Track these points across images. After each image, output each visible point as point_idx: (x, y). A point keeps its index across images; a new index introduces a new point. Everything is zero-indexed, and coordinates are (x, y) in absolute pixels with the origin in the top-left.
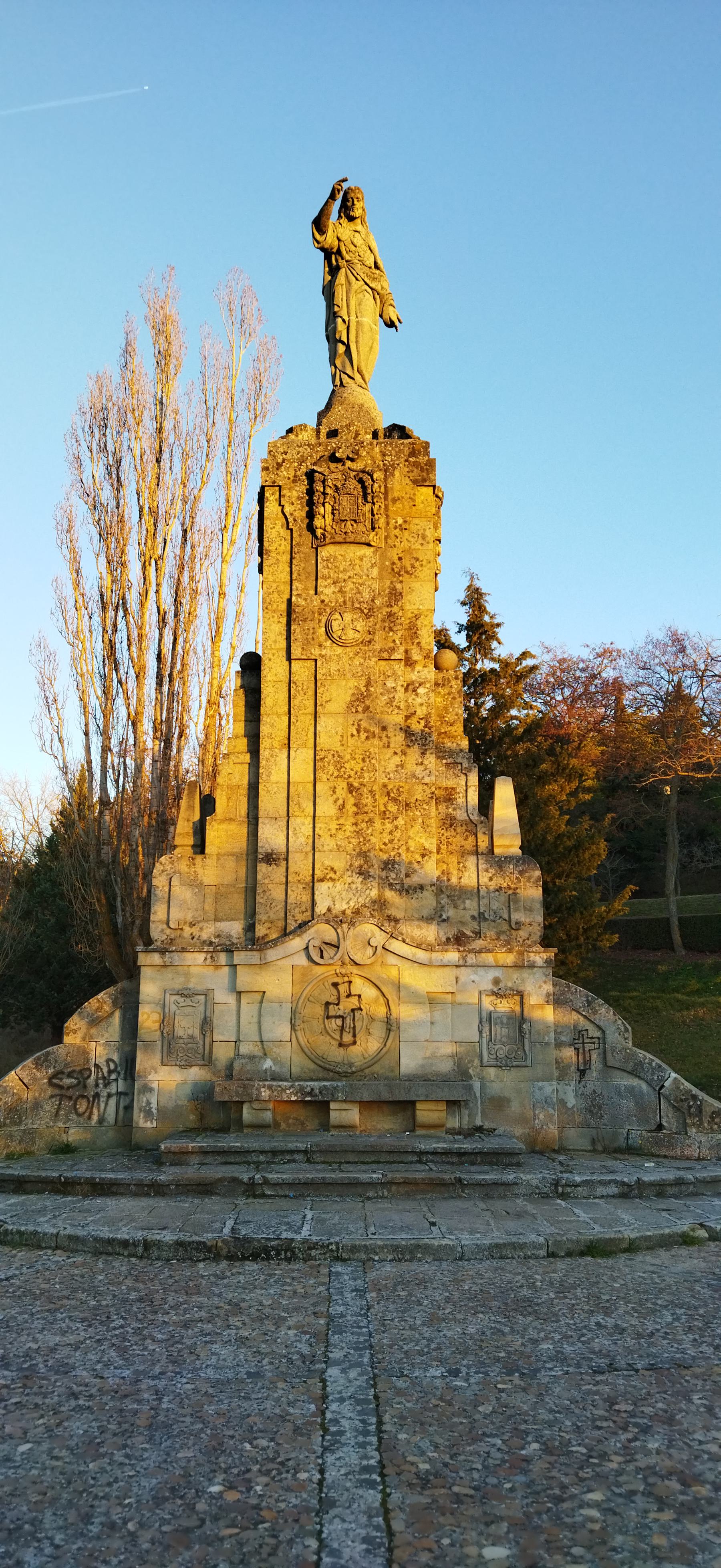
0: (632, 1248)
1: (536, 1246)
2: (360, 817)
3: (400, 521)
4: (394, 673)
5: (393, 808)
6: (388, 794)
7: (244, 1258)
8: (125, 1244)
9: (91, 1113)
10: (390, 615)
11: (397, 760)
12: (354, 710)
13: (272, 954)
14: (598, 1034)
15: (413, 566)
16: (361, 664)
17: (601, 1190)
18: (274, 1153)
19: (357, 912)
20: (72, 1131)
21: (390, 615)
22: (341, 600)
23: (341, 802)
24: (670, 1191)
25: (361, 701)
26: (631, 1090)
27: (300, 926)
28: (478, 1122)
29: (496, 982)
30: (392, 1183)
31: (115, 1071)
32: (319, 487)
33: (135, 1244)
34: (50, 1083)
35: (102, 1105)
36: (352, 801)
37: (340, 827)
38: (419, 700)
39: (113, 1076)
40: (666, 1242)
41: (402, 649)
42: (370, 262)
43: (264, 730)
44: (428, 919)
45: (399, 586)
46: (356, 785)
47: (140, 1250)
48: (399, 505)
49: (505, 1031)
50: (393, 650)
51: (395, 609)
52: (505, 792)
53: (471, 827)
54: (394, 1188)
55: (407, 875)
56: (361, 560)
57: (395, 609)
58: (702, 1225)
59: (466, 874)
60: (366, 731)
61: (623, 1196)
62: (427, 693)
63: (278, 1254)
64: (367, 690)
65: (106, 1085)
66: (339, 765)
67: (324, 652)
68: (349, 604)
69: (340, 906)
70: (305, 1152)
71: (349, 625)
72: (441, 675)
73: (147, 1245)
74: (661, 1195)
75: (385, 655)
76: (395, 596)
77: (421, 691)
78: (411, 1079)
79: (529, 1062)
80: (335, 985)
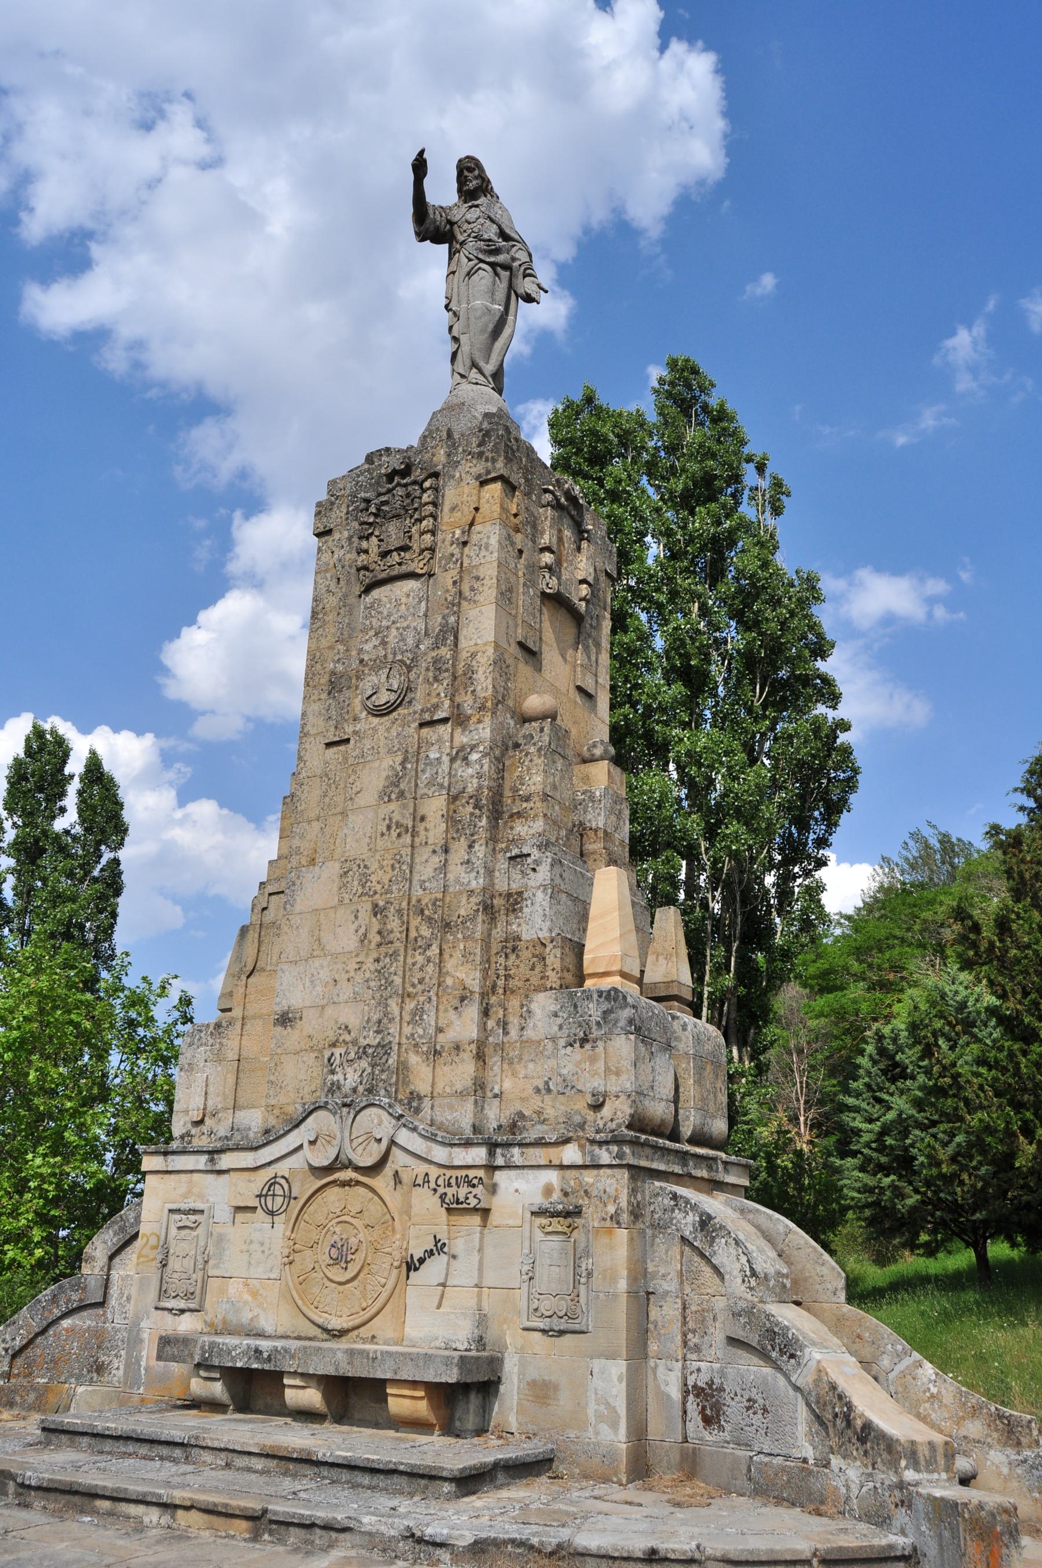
2: (383, 950)
11: (436, 860)
15: (472, 589)
16: (399, 734)
23: (362, 930)
25: (394, 788)
36: (376, 926)
46: (381, 903)
50: (436, 707)
53: (539, 949)
60: (398, 825)
64: (404, 768)
75: (427, 717)
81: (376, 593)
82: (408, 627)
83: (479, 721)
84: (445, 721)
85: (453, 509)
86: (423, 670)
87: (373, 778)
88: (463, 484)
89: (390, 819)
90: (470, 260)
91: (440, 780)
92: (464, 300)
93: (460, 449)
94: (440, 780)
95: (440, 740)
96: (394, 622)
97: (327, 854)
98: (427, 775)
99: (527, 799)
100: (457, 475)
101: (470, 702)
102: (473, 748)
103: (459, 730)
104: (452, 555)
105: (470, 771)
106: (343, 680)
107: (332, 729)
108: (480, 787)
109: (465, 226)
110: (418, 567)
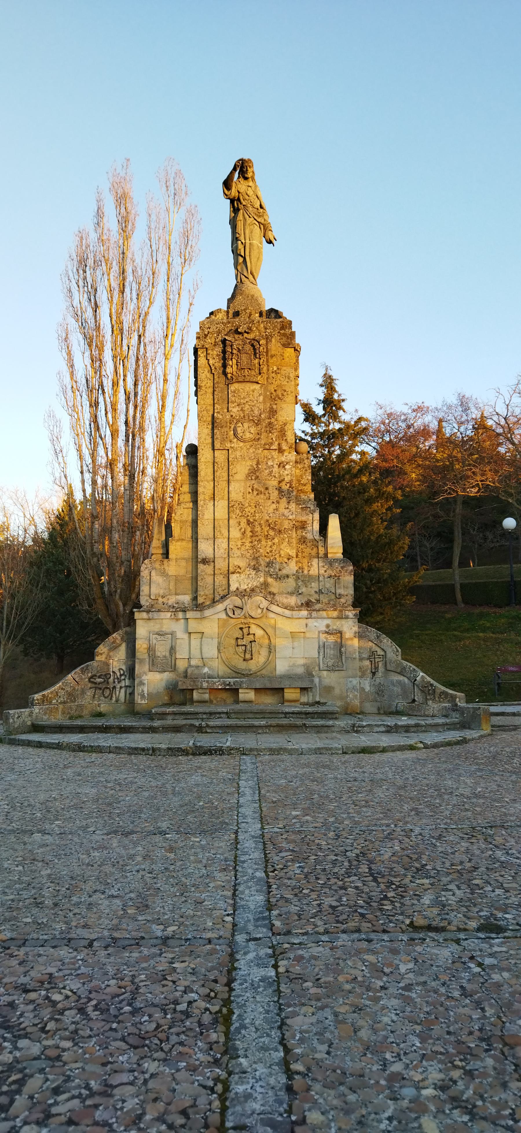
0: (384, 750)
1: (336, 749)
2: (254, 538)
3: (275, 368)
4: (272, 457)
5: (272, 533)
6: (269, 525)
7: (200, 754)
8: (143, 749)
9: (112, 696)
10: (270, 423)
11: (274, 506)
13: (207, 613)
14: (382, 653)
15: (283, 395)
17: (376, 729)
18: (211, 714)
19: (253, 590)
20: (102, 706)
21: (270, 423)
22: (242, 415)
23: (243, 530)
24: (412, 729)
25: (254, 473)
26: (399, 682)
27: (222, 598)
28: (318, 699)
29: (328, 626)
30: (271, 726)
31: (123, 674)
32: (229, 349)
33: (148, 750)
34: (90, 681)
35: (118, 693)
36: (249, 529)
37: (243, 544)
38: (286, 472)
39: (123, 677)
40: (401, 748)
41: (276, 443)
42: (258, 205)
43: (200, 490)
44: (291, 594)
45: (275, 407)
47: (151, 752)
48: (274, 359)
49: (332, 652)
50: (272, 444)
51: (273, 420)
52: (334, 522)
53: (315, 543)
54: (272, 728)
55: (280, 570)
57: (273, 420)
58: (421, 742)
59: (312, 569)
60: (257, 490)
61: (388, 732)
62: (291, 469)
63: (216, 752)
65: (119, 682)
66: (242, 510)
68: (247, 417)
69: (244, 587)
70: (227, 713)
71: (247, 430)
72: (299, 457)
73: (154, 750)
74: (407, 731)
75: (267, 447)
76: (273, 412)
77: (287, 467)
78: (282, 677)
79: (344, 668)
80: (241, 629)
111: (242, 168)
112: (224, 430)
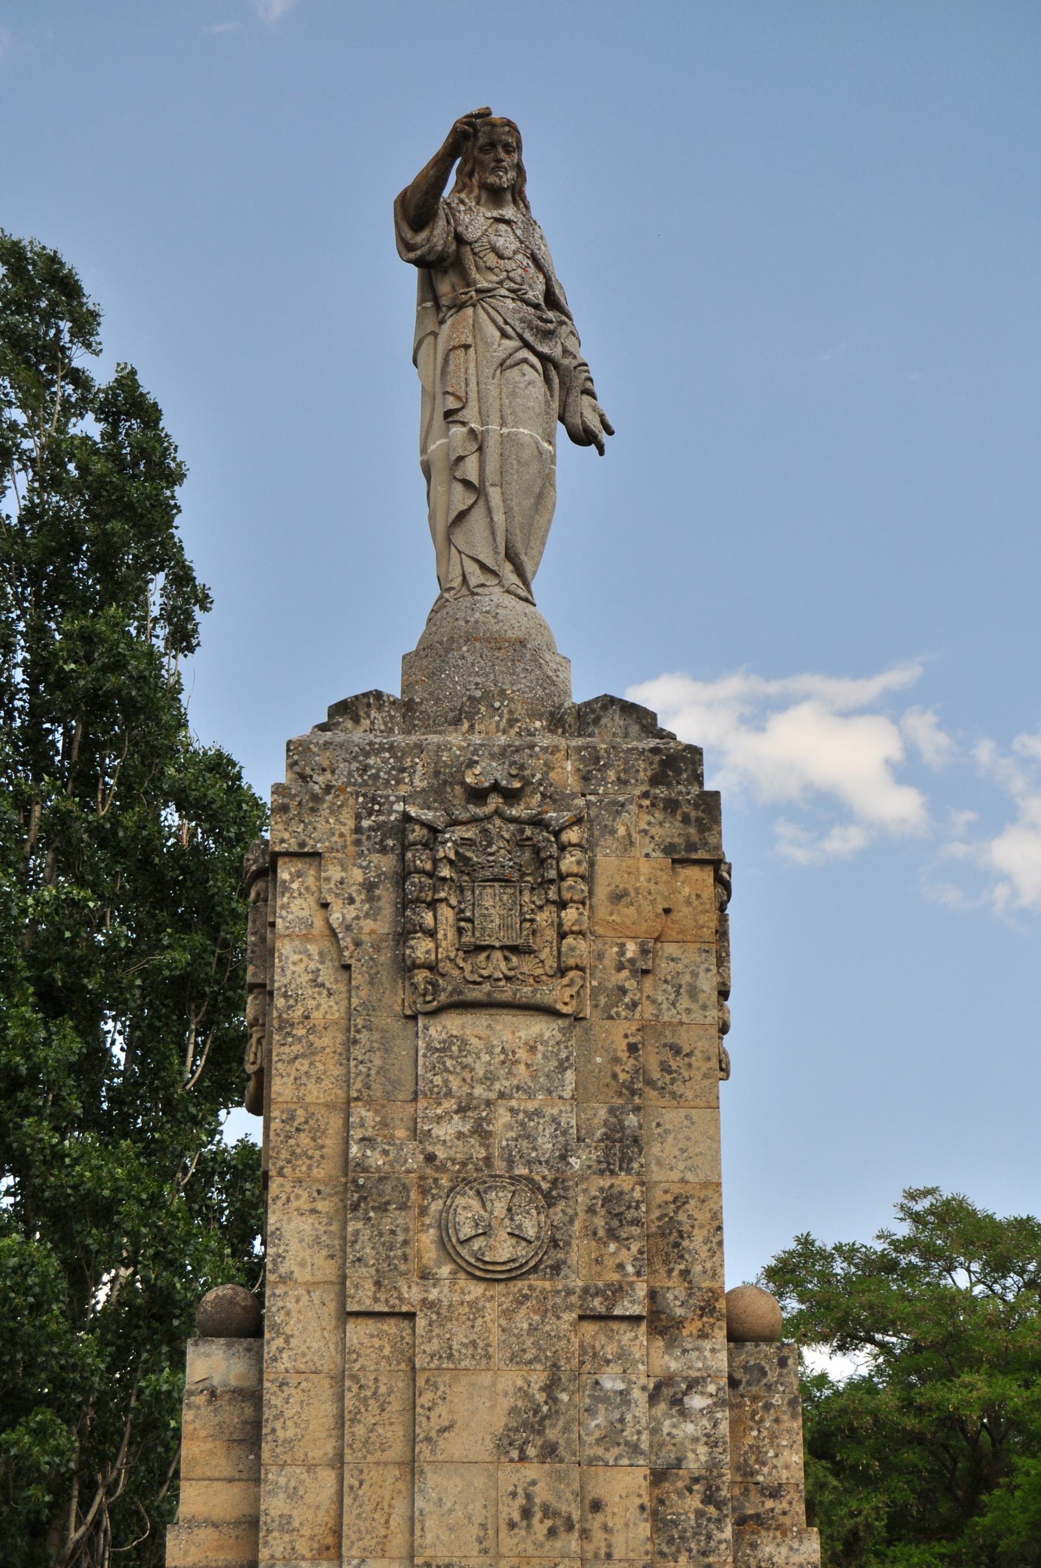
12: (515, 1454)
15: (666, 1068)
16: (533, 1329)
25: (530, 1433)
41: (641, 1290)
42: (536, 292)
50: (618, 1290)
56: (532, 1049)
60: (547, 1511)
62: (709, 1412)
64: (552, 1399)
67: (433, 1294)
68: (500, 1166)
75: (598, 1305)
76: (622, 1147)
81: (453, 1024)
82: (538, 1113)
83: (703, 1335)
84: (636, 1319)
85: (618, 897)
86: (581, 1209)
87: (478, 1407)
88: (637, 852)
89: (529, 1496)
90: (504, 335)
91: (629, 1434)
92: (495, 416)
93: (612, 775)
94: (629, 1434)
95: (622, 1355)
96: (502, 1095)
97: (369, 1542)
98: (600, 1420)
99: (775, 1493)
100: (622, 831)
101: (680, 1292)
102: (693, 1384)
103: (660, 1343)
104: (623, 991)
105: (690, 1428)
106: (388, 1188)
107: (369, 1285)
108: (713, 1465)
109: (491, 259)
110: (557, 993)
111: (481, 150)
112: (394, 1218)
